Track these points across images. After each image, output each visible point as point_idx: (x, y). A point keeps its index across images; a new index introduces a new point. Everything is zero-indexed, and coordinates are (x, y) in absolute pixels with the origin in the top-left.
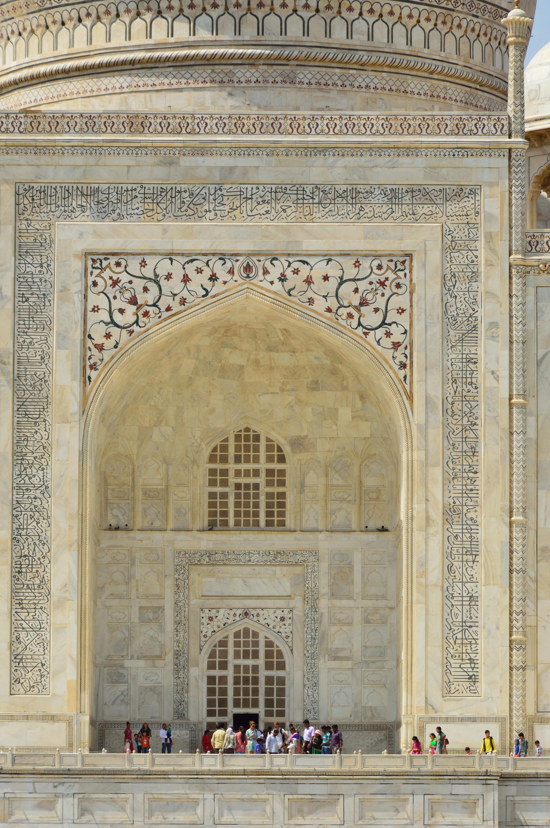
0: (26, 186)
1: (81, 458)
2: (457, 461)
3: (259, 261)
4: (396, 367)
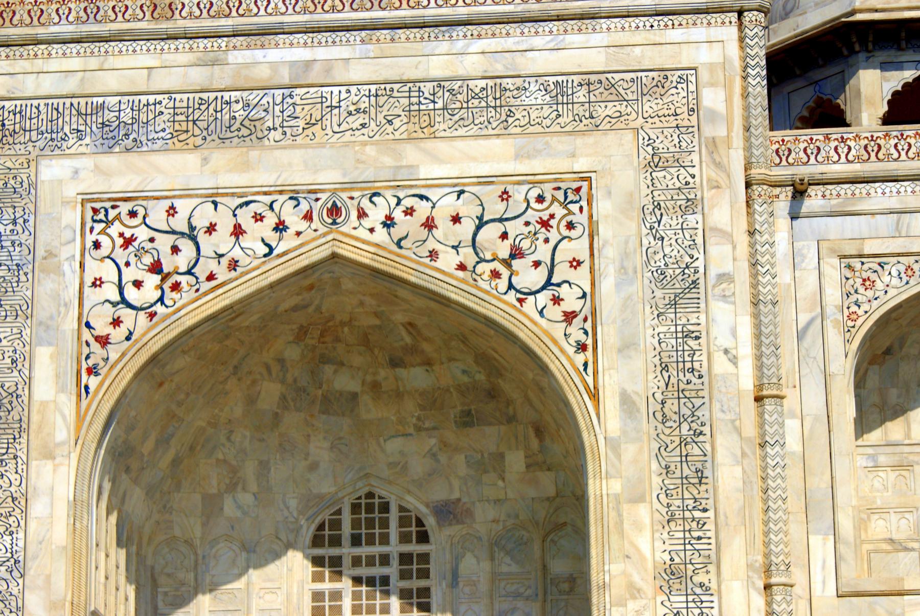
1: (71, 513)
2: (674, 492)
3: (352, 198)
4: (571, 350)
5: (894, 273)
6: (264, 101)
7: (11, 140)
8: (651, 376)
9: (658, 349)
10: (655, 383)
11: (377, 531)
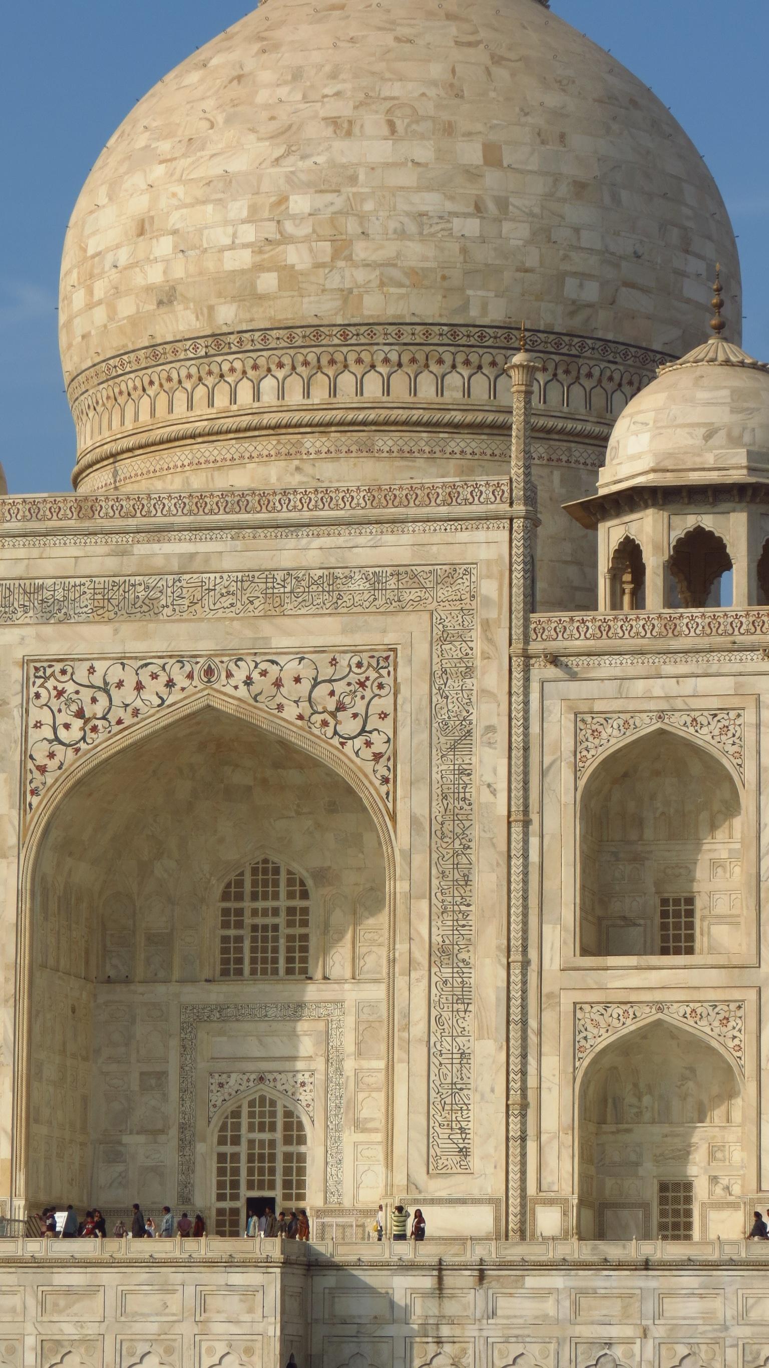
2: (447, 891)
3: (222, 662)
4: (377, 783)
5: (615, 726)
6: (159, 585)
9: (441, 783)
10: (438, 809)
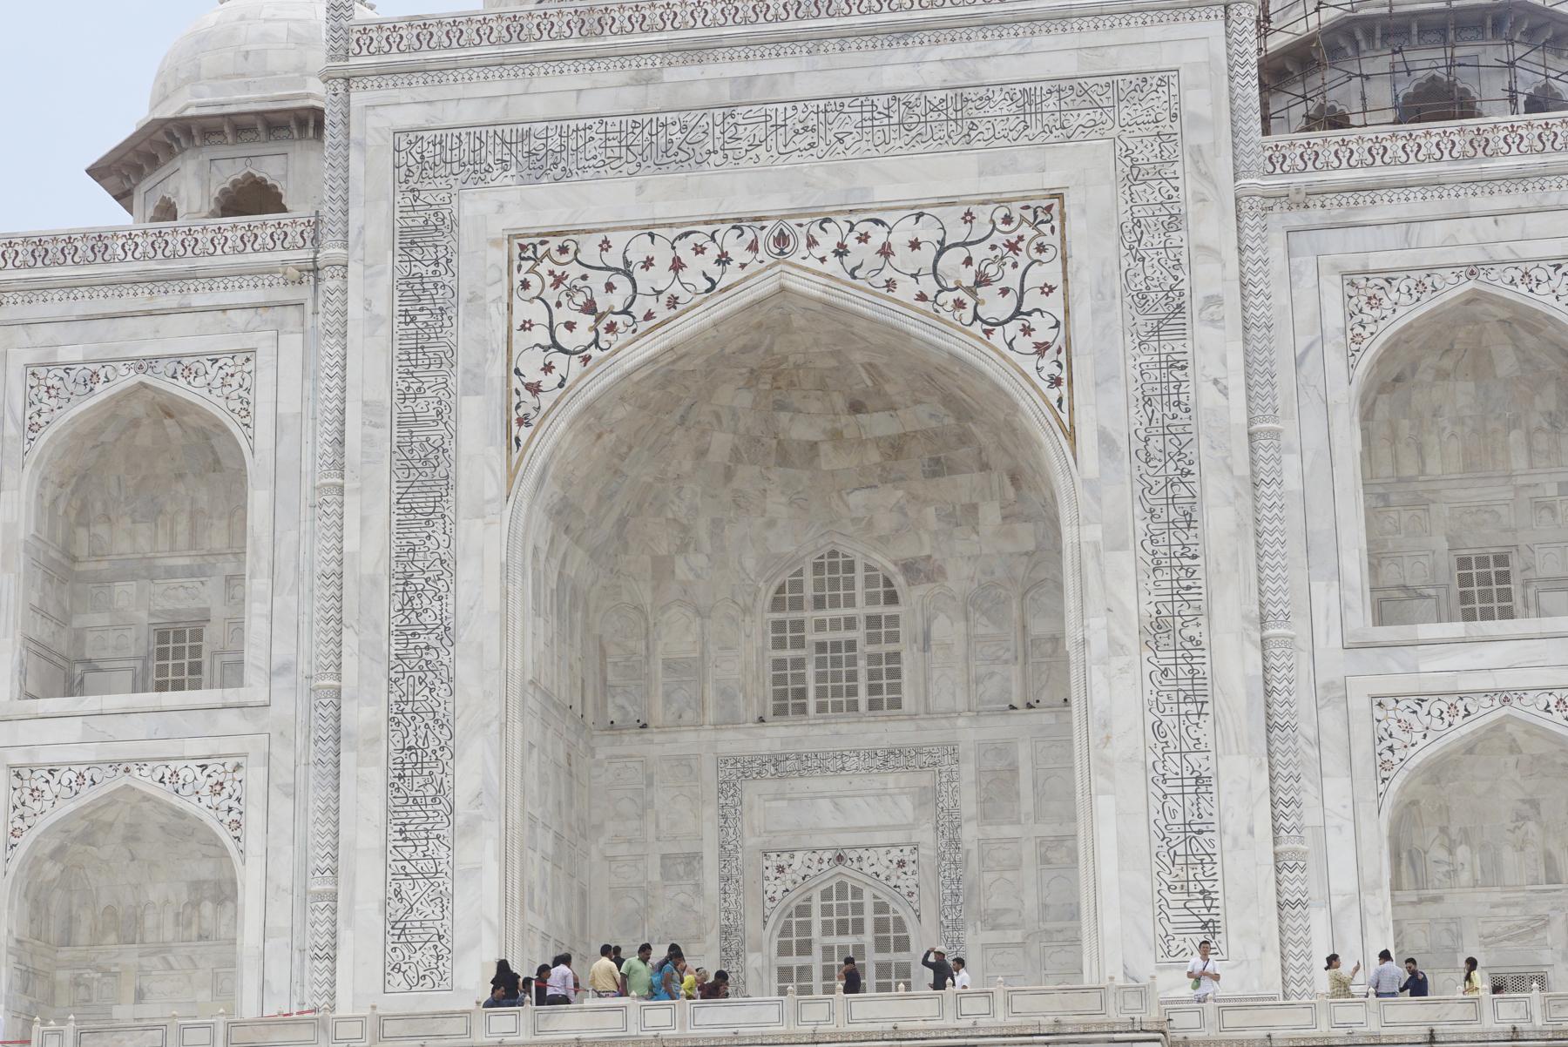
0: (412, 137)
2: (1160, 538)
3: (800, 225)
4: (1044, 386)
5: (1404, 289)
6: (703, 122)
7: (431, 173)
8: (1133, 411)
10: (1138, 417)
11: (842, 592)
